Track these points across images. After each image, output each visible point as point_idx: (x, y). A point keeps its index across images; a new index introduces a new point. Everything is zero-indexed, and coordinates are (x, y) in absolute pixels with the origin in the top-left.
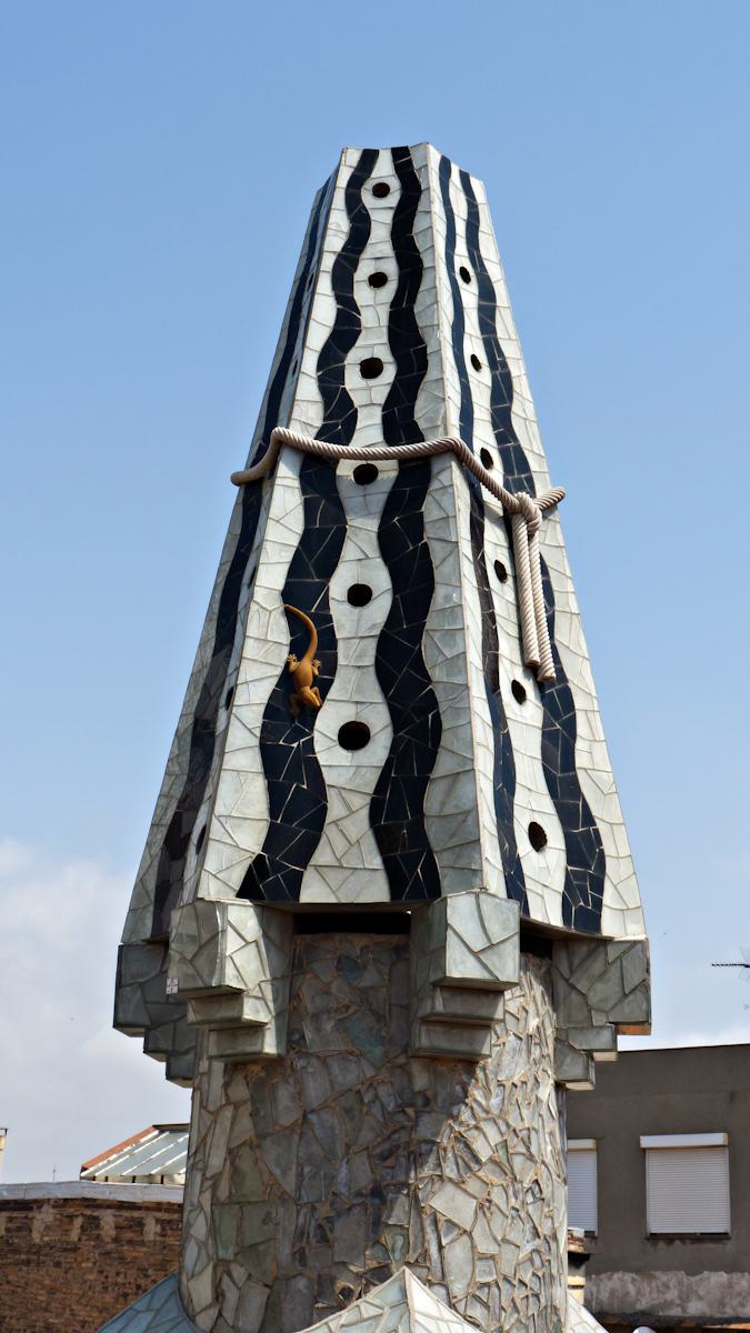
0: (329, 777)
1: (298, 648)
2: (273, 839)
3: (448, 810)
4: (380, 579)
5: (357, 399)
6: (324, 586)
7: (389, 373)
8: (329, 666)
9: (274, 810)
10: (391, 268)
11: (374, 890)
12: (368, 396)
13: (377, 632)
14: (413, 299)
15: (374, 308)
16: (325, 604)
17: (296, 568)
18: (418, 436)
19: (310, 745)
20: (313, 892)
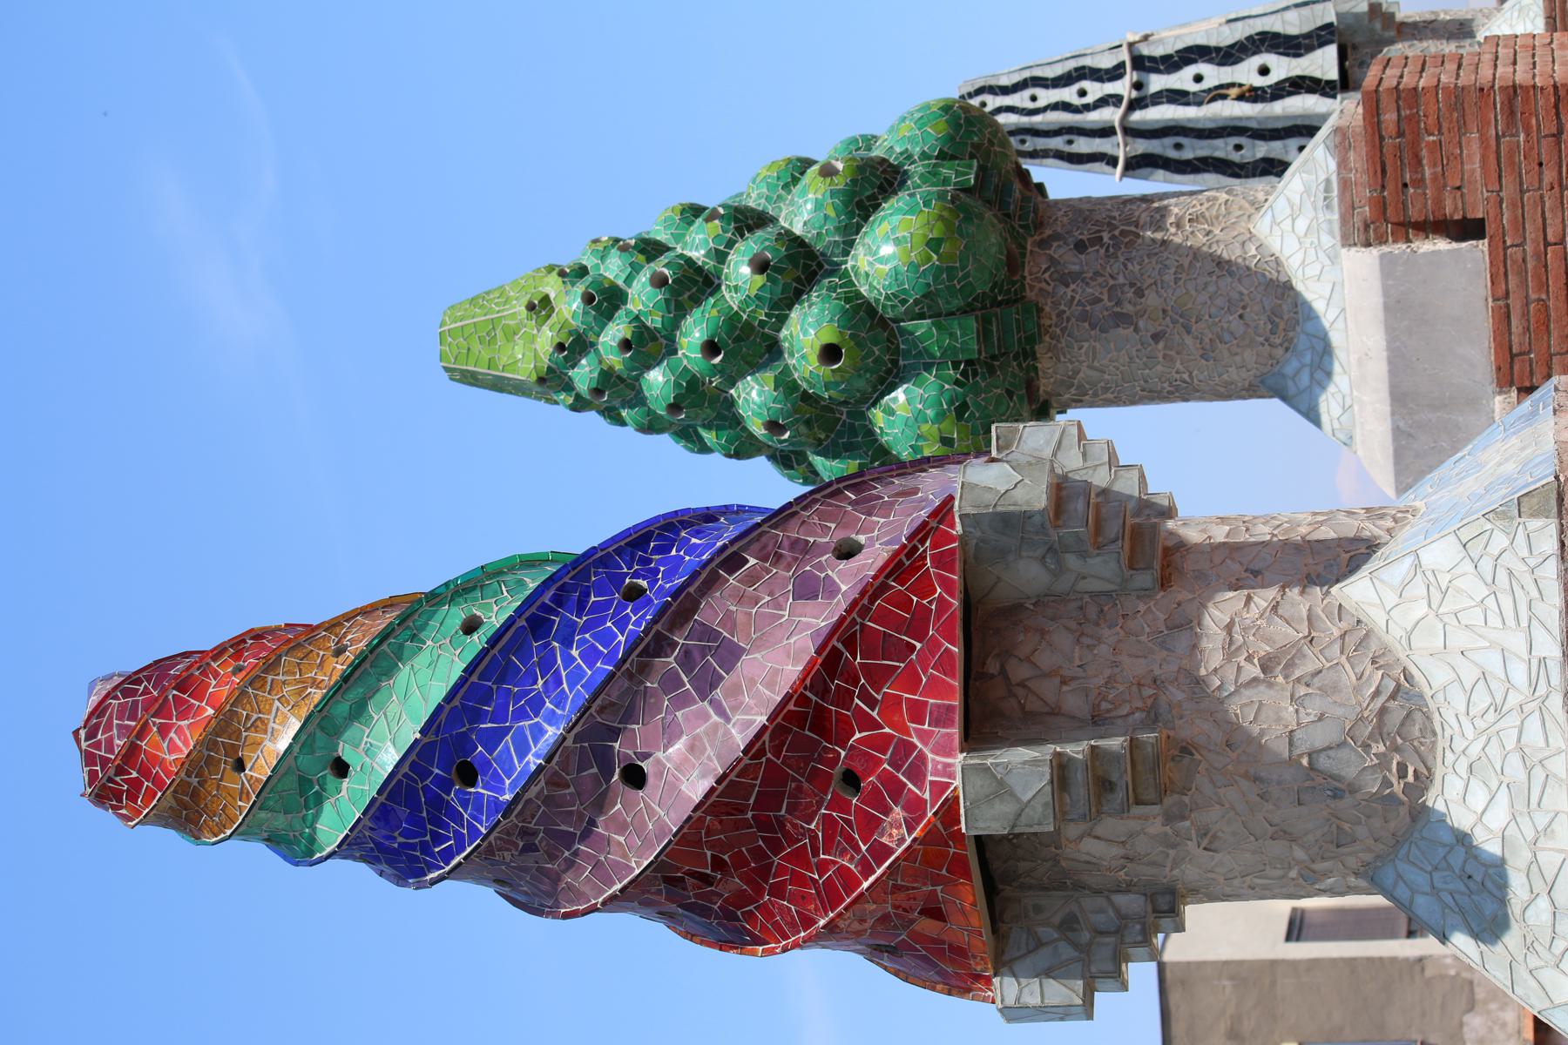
0: (1283, 76)
1: (1224, 97)
2: (1311, 91)
3: (1297, 23)
4: (1189, 71)
5: (1098, 95)
6: (1194, 93)
7: (1086, 84)
8: (1232, 85)
9: (1300, 93)
10: (1027, 93)
11: (1331, 51)
12: (1096, 90)
13: (1216, 67)
14: (1046, 79)
15: (1046, 96)
16: (1204, 91)
17: (1187, 104)
18: (1121, 65)
19: (1269, 87)
20: (1333, 74)
